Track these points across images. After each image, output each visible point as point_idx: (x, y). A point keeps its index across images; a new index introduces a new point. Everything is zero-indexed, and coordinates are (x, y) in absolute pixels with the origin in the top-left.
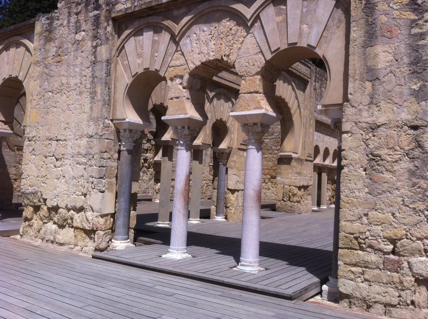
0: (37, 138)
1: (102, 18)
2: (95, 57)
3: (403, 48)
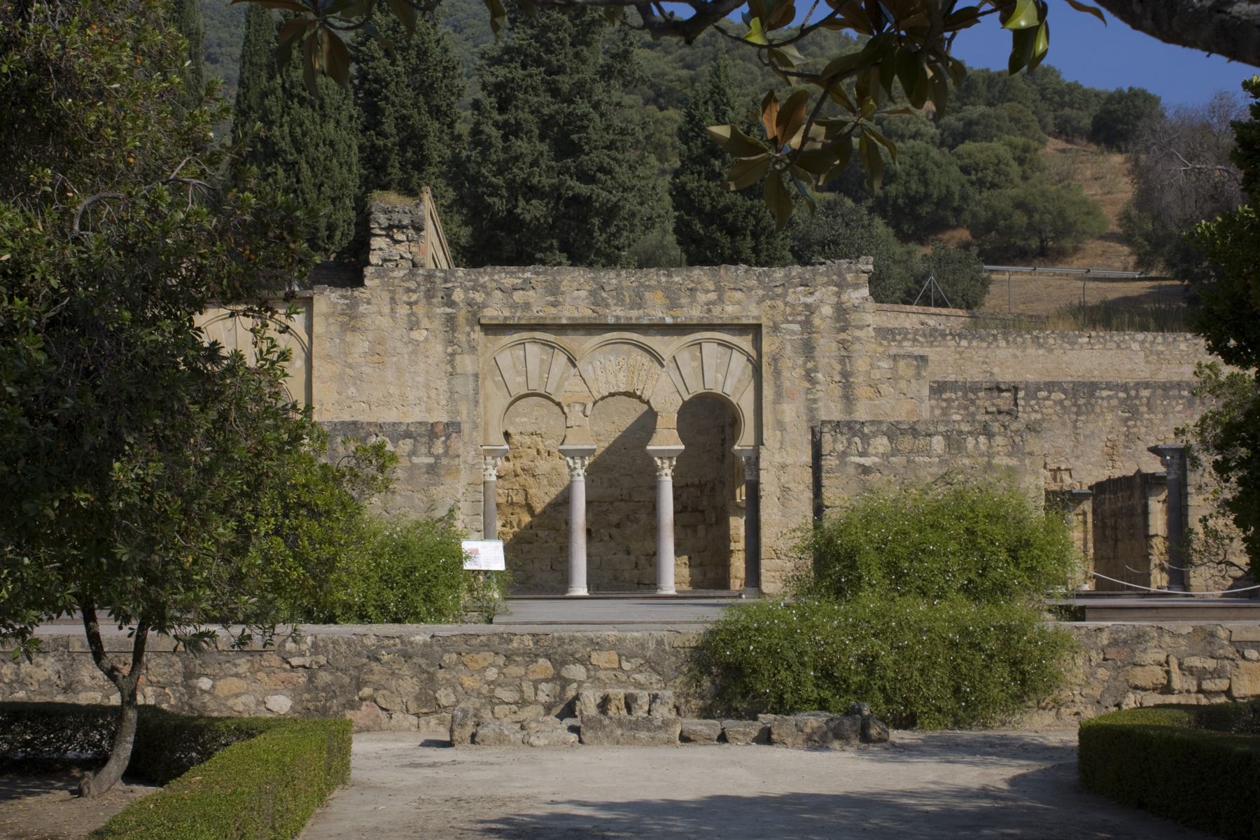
1: (461, 320)
2: (453, 367)
3: (802, 409)
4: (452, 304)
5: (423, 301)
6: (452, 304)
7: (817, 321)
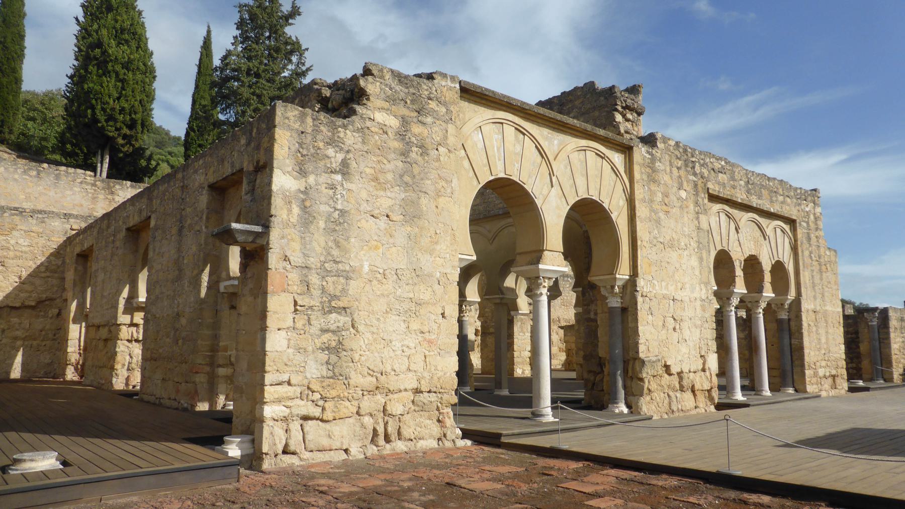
4: (695, 174)
5: (683, 168)
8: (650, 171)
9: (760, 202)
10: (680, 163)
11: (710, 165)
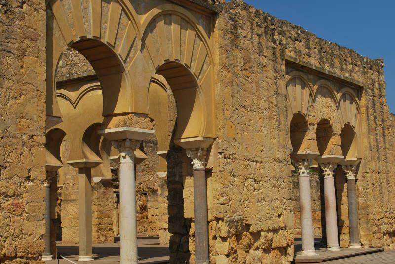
0: (235, 156)
4: (274, 41)
6: (274, 41)
7: (375, 90)
8: (233, 37)
9: (332, 69)
10: (261, 30)
11: (288, 34)
